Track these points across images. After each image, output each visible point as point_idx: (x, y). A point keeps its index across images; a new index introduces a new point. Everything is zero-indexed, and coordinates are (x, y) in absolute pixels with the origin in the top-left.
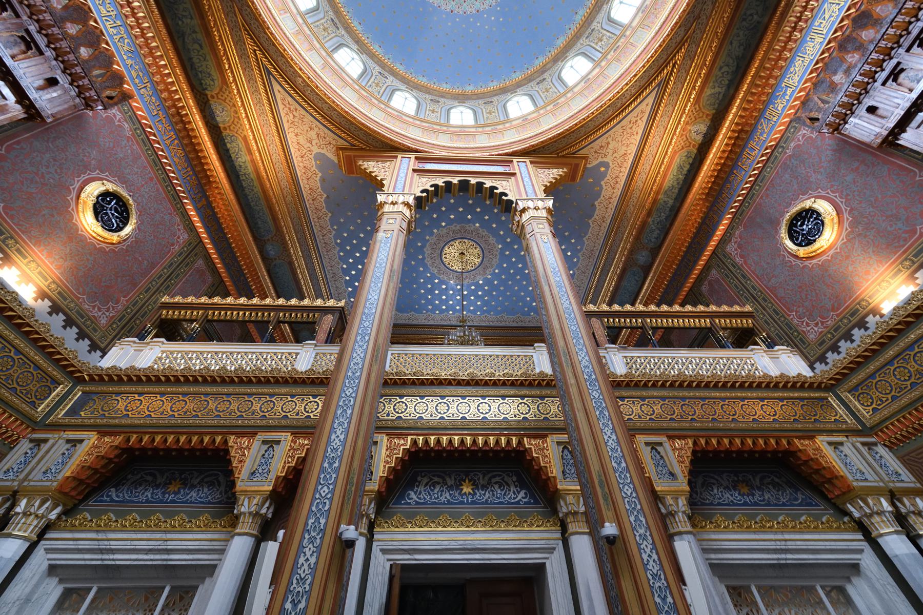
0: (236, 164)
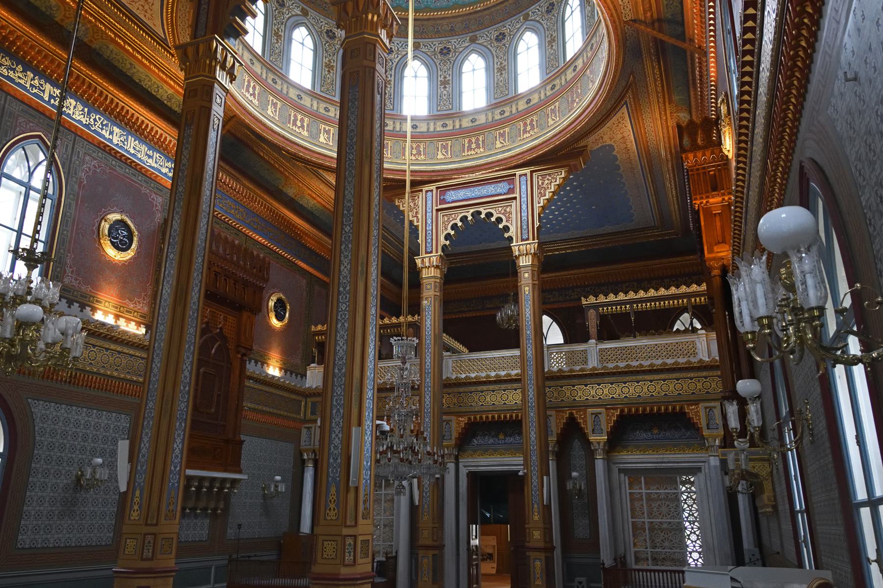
0: (309, 208)
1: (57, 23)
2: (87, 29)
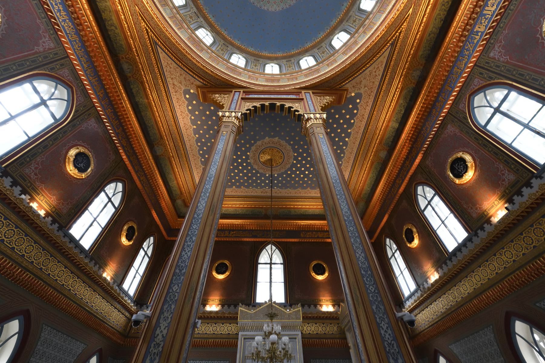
1: (416, 85)
2: (414, 71)
